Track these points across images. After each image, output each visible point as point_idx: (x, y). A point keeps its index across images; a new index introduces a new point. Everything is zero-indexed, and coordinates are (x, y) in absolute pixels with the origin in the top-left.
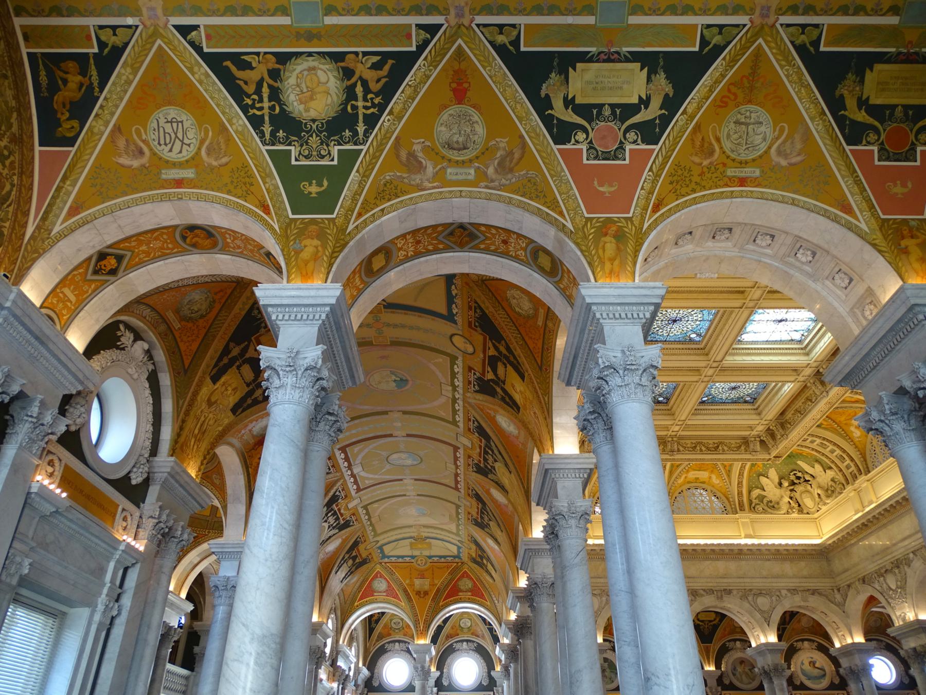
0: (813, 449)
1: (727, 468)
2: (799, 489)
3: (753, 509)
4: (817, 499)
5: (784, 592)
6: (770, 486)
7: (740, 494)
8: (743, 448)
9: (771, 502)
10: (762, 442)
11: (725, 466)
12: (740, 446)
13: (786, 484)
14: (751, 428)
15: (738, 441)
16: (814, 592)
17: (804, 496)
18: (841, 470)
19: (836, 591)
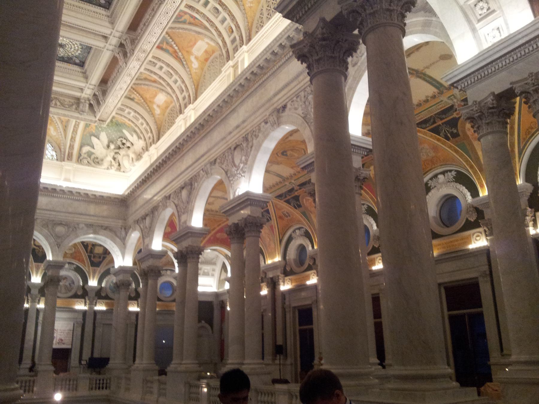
0: (129, 120)
1: (64, 123)
2: (122, 152)
3: (79, 160)
4: (131, 161)
5: (81, 226)
6: (99, 146)
7: (72, 147)
8: (74, 107)
9: (97, 158)
10: (91, 105)
11: (62, 122)
12: (72, 105)
13: (112, 146)
14: (82, 90)
15: (73, 101)
16: (106, 228)
17: (124, 158)
18: (145, 140)
19: (123, 229)
